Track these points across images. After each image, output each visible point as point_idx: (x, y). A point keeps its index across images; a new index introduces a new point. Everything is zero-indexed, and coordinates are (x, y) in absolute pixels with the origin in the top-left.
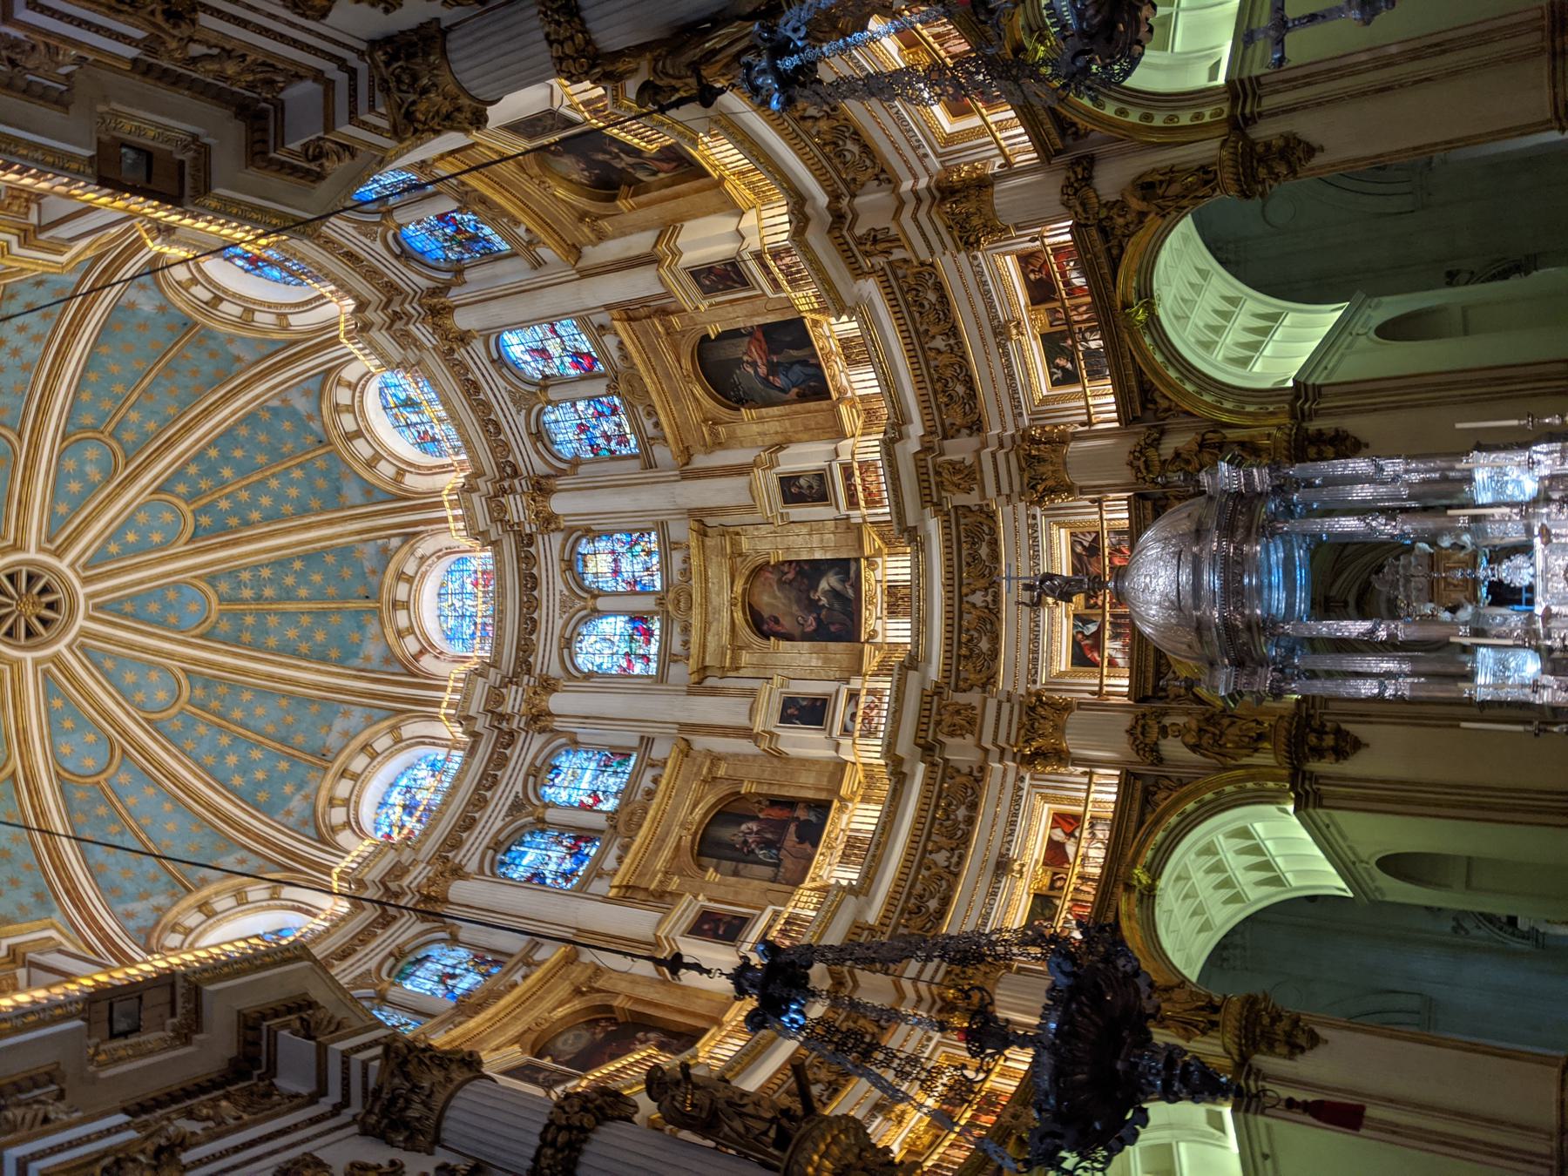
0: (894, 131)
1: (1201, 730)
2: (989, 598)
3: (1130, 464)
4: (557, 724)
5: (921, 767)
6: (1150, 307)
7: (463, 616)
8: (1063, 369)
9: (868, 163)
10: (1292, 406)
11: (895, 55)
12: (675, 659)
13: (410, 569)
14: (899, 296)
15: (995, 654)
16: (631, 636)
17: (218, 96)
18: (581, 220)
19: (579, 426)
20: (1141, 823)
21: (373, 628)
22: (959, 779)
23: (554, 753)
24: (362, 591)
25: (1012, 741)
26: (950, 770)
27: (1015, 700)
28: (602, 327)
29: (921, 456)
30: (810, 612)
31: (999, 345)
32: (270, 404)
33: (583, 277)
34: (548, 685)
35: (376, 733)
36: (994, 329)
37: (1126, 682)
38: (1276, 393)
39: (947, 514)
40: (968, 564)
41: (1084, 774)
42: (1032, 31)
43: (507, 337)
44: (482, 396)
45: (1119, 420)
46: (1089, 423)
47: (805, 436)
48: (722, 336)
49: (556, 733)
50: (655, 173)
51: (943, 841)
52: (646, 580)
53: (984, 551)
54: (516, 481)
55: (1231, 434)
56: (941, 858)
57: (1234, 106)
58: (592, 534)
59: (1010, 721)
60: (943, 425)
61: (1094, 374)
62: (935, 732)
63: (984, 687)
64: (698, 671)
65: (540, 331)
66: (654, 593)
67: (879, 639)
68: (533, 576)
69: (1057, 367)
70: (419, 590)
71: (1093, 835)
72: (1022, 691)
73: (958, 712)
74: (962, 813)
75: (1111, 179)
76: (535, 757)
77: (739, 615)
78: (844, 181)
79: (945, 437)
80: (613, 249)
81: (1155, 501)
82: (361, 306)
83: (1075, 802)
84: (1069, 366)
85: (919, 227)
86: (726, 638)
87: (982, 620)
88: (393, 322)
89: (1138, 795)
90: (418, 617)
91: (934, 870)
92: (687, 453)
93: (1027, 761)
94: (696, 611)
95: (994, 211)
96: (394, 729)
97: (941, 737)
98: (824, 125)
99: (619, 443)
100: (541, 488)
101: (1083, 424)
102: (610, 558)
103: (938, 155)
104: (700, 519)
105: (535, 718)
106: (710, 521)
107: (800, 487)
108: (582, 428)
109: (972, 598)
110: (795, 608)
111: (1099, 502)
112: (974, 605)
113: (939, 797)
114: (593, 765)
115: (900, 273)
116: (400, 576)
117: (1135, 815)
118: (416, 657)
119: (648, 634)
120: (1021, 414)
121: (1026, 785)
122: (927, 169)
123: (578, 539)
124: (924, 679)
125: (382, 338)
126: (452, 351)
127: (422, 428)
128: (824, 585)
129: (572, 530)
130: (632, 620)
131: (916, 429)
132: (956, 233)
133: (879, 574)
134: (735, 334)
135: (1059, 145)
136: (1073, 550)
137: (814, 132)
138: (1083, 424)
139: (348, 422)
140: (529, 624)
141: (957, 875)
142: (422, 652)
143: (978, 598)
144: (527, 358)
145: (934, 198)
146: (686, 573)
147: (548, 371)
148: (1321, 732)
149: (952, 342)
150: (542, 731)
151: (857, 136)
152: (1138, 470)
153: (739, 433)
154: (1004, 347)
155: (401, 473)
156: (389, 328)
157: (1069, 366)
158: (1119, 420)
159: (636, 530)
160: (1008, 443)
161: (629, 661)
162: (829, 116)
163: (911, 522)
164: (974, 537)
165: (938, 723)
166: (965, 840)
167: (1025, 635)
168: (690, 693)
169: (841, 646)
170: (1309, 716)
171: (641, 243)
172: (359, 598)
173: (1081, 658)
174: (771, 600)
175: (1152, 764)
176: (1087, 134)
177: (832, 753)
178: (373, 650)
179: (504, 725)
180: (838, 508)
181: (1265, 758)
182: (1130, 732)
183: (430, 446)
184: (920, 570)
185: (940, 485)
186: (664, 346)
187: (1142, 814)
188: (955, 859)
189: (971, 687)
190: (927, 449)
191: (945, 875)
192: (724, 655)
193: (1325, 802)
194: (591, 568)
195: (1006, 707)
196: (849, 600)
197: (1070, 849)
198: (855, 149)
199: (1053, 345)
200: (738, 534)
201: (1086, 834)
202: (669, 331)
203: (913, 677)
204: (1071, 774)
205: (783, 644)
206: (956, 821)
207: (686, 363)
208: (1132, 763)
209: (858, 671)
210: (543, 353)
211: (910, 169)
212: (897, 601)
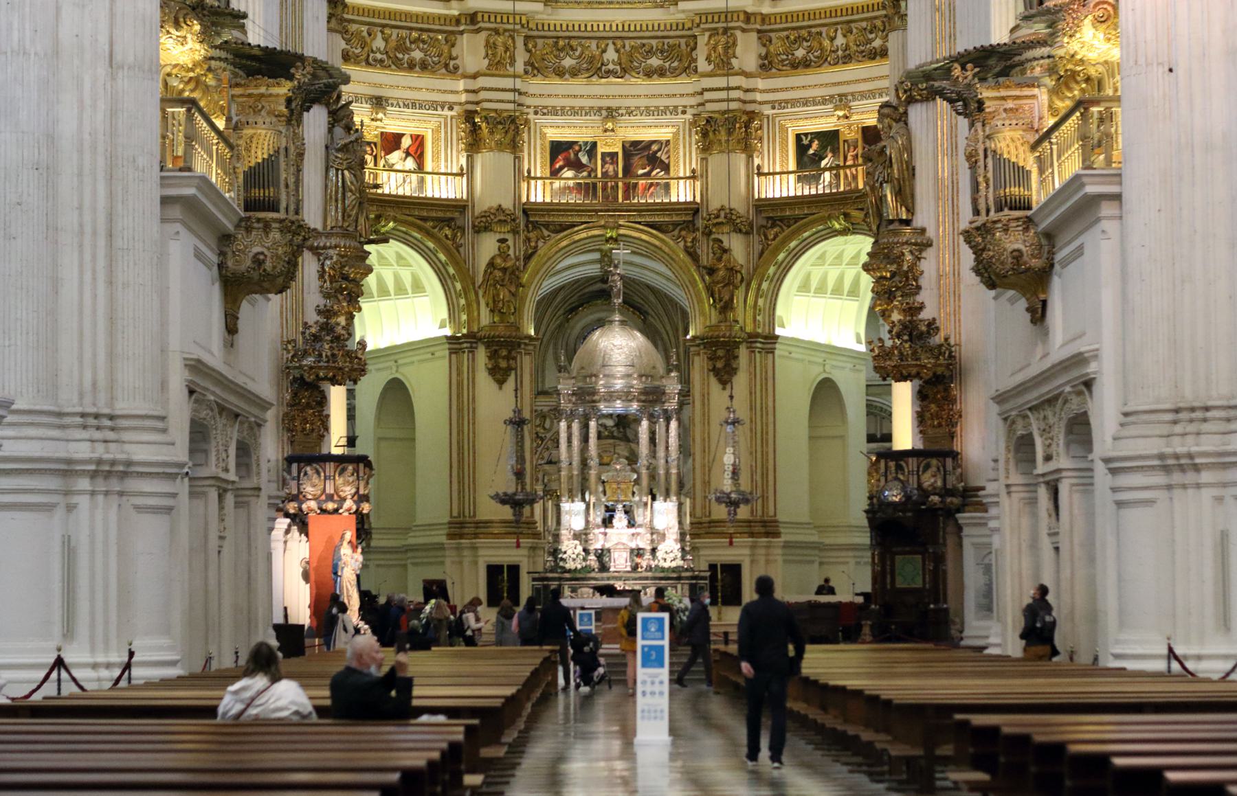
1: (504, 270)
2: (611, 67)
3: (722, 208)
5: (456, 13)
6: (844, 232)
8: (809, 146)
10: (757, 335)
15: (560, 73)
20: (424, 219)
22: (446, 49)
29: (742, 17)
31: (832, 97)
36: (845, 95)
37: (540, 200)
41: (462, 169)
45: (759, 199)
46: (760, 174)
51: (393, 44)
53: (655, 62)
55: (739, 294)
56: (379, 43)
59: (502, 101)
61: (799, 179)
63: (532, 65)
69: (811, 142)
72: (528, 101)
73: (507, 49)
74: (417, 55)
79: (759, 31)
81: (692, 222)
83: (436, 156)
84: (811, 151)
87: (591, 60)
89: (449, 215)
91: (368, 40)
93: (469, 116)
97: (484, 35)
101: (759, 167)
109: (611, 48)
111: (693, 177)
112: (604, 51)
120: (773, 108)
121: (447, 112)
138: (759, 167)
141: (368, 64)
143: (611, 55)
152: (718, 216)
154: (831, 102)
157: (811, 151)
160: (749, 96)
164: (668, 52)
165: (497, 32)
166: (398, 64)
167: (577, 103)
170: (519, 345)
173: (558, 149)
175: (474, 226)
181: (485, 318)
182: (499, 208)
187: (433, 219)
188: (379, 56)
189: (529, 51)
191: (366, 49)
193: (454, 356)
197: (395, 157)
199: (830, 139)
204: (458, 152)
206: (407, 50)
208: (473, 207)
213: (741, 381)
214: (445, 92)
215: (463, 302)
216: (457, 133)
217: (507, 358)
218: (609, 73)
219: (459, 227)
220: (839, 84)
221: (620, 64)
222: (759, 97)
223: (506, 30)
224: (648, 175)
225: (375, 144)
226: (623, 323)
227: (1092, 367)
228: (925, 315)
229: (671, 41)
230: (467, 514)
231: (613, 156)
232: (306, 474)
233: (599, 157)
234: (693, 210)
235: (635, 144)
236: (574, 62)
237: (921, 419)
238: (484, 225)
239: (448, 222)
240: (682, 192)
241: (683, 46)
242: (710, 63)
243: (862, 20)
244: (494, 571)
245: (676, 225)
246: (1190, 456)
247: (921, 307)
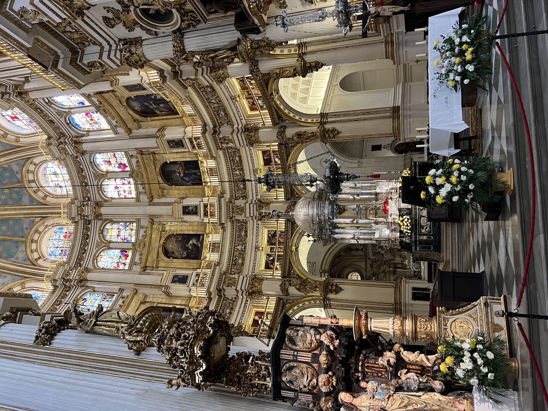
0: (235, 111)
1: (300, 284)
2: (243, 248)
4: (89, 284)
7: (57, 247)
9: (226, 118)
11: (239, 90)
12: (135, 264)
13: (41, 230)
14: (228, 157)
15: (243, 264)
17: (67, 44)
18: (135, 121)
21: (22, 248)
24: (21, 235)
25: (246, 288)
26: (226, 299)
27: (248, 276)
28: (132, 156)
30: (185, 251)
31: (254, 174)
32: (4, 166)
33: (130, 139)
34: (87, 270)
35: (16, 284)
36: (253, 170)
37: (280, 272)
39: (233, 221)
40: (238, 237)
42: (275, 91)
43: (98, 155)
44: (84, 174)
45: (285, 199)
47: (193, 196)
48: (170, 162)
49: (88, 287)
50: (161, 112)
53: (243, 234)
54: (89, 202)
57: (321, 119)
58: (112, 222)
59: (246, 282)
60: (235, 195)
62: (223, 286)
63: (239, 273)
64: (144, 267)
65: (110, 155)
66: (131, 243)
67: (207, 259)
68: (88, 235)
70: (43, 237)
71: (267, 318)
73: (231, 280)
74: (228, 311)
75: (290, 132)
76: (78, 295)
77: (161, 250)
78: (218, 122)
79: (235, 200)
80: (142, 132)
82: (49, 138)
83: (262, 307)
85: (238, 138)
86: (155, 257)
87: (240, 254)
88: (59, 145)
90: (40, 246)
92: (152, 198)
94: (146, 248)
95: (258, 136)
96: (23, 283)
98: (216, 105)
99: (128, 194)
100: (98, 205)
102: (117, 231)
103: (245, 119)
104: (152, 219)
105: (81, 281)
106: (155, 220)
107: (189, 210)
108: (116, 188)
110: (180, 249)
112: (238, 249)
113: (221, 306)
114: (100, 298)
115: (229, 151)
116: (37, 231)
117: (280, 310)
118: (36, 260)
119: (126, 256)
120: (258, 195)
121: (248, 303)
122: (242, 123)
123: (107, 223)
124: (221, 269)
125: (54, 149)
126: (77, 157)
127: (57, 183)
128: (191, 242)
129: (106, 220)
130: (121, 251)
131: (227, 196)
132: (247, 141)
133: (210, 239)
134: (175, 163)
135: (278, 122)
136: (268, 236)
137: (212, 107)
139: (31, 177)
140: (83, 251)
144: (103, 163)
145: (242, 131)
146: (144, 236)
148: (332, 286)
149: (241, 172)
151: (225, 110)
153: (171, 193)
155: (46, 196)
156: (58, 146)
158: (285, 199)
159: (128, 222)
160: (254, 202)
162: (218, 103)
163: (223, 222)
167: (253, 259)
168: (140, 274)
169: (195, 260)
171: (153, 131)
172: (19, 237)
173: (267, 267)
174: (172, 246)
175: (286, 295)
176: (285, 121)
177: (188, 293)
178: (20, 255)
180: (200, 217)
181: (317, 294)
183: (59, 189)
184: (223, 238)
185: (233, 212)
186: (152, 164)
189: (234, 274)
190: (230, 202)
192: (154, 263)
193: (332, 307)
194: (109, 234)
195: (245, 278)
196: (199, 247)
198: (223, 114)
200: (164, 224)
201: (265, 318)
202: (155, 160)
203: (218, 267)
204: (262, 299)
205: (175, 260)
207: (158, 170)
208: (280, 295)
209: (199, 268)
211: (237, 122)
212: (215, 247)
214: (242, 302)
215: (312, 302)
216: (256, 299)
217: (332, 286)
218: (245, 249)
219: (287, 301)
220: (250, 172)
221: (243, 245)
222: (255, 199)
223: (224, 280)
225: (255, 329)
226: (293, 211)
229: (237, 228)
230: (392, 307)
231: (271, 249)
232: (291, 382)
233: (271, 253)
235: (268, 242)
236: (240, 259)
238: (285, 291)
239: (284, 305)
241: (239, 224)
242: (242, 214)
243: (231, 165)
244: (416, 297)
245: (292, 227)
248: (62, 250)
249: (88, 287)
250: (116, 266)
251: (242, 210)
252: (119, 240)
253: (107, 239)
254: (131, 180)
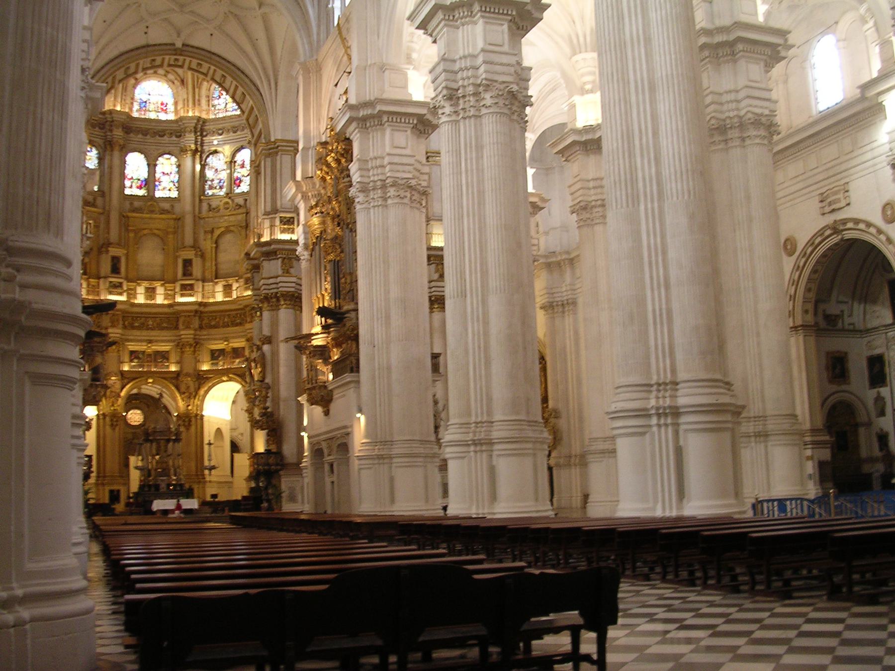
16: (139, 180)
19: (217, 170)
23: (97, 149)
38: (202, 410)
49: (105, 150)
52: (160, 188)
53: (165, 325)
58: (179, 166)
76: (95, 142)
79: (200, 317)
111: (178, 363)
119: (140, 188)
130: (146, 180)
131: (202, 309)
142: (136, 79)
143: (150, 323)
147: (236, 164)
150: (106, 147)
161: (130, 179)
173: (132, 352)
179: (108, 127)
183: (216, 94)
190: (196, 311)
199: (222, 352)
210: (243, 166)
213: (193, 428)
224: (161, 362)
227: (350, 430)
228: (269, 410)
231: (151, 355)
234: (178, 374)
237: (268, 442)
240: (173, 368)
246: (382, 455)
247: (268, 408)
248: (146, 102)
249: (105, 150)
250: (129, 177)
251: (188, 327)
252: (157, 175)
253: (160, 159)
254: (224, 190)
